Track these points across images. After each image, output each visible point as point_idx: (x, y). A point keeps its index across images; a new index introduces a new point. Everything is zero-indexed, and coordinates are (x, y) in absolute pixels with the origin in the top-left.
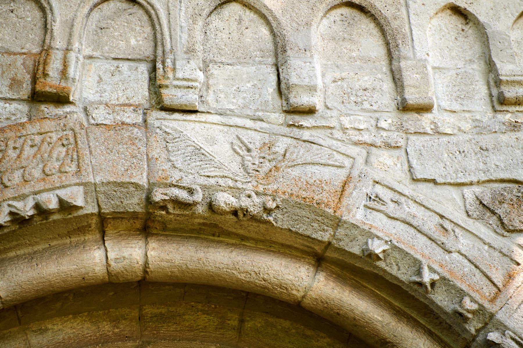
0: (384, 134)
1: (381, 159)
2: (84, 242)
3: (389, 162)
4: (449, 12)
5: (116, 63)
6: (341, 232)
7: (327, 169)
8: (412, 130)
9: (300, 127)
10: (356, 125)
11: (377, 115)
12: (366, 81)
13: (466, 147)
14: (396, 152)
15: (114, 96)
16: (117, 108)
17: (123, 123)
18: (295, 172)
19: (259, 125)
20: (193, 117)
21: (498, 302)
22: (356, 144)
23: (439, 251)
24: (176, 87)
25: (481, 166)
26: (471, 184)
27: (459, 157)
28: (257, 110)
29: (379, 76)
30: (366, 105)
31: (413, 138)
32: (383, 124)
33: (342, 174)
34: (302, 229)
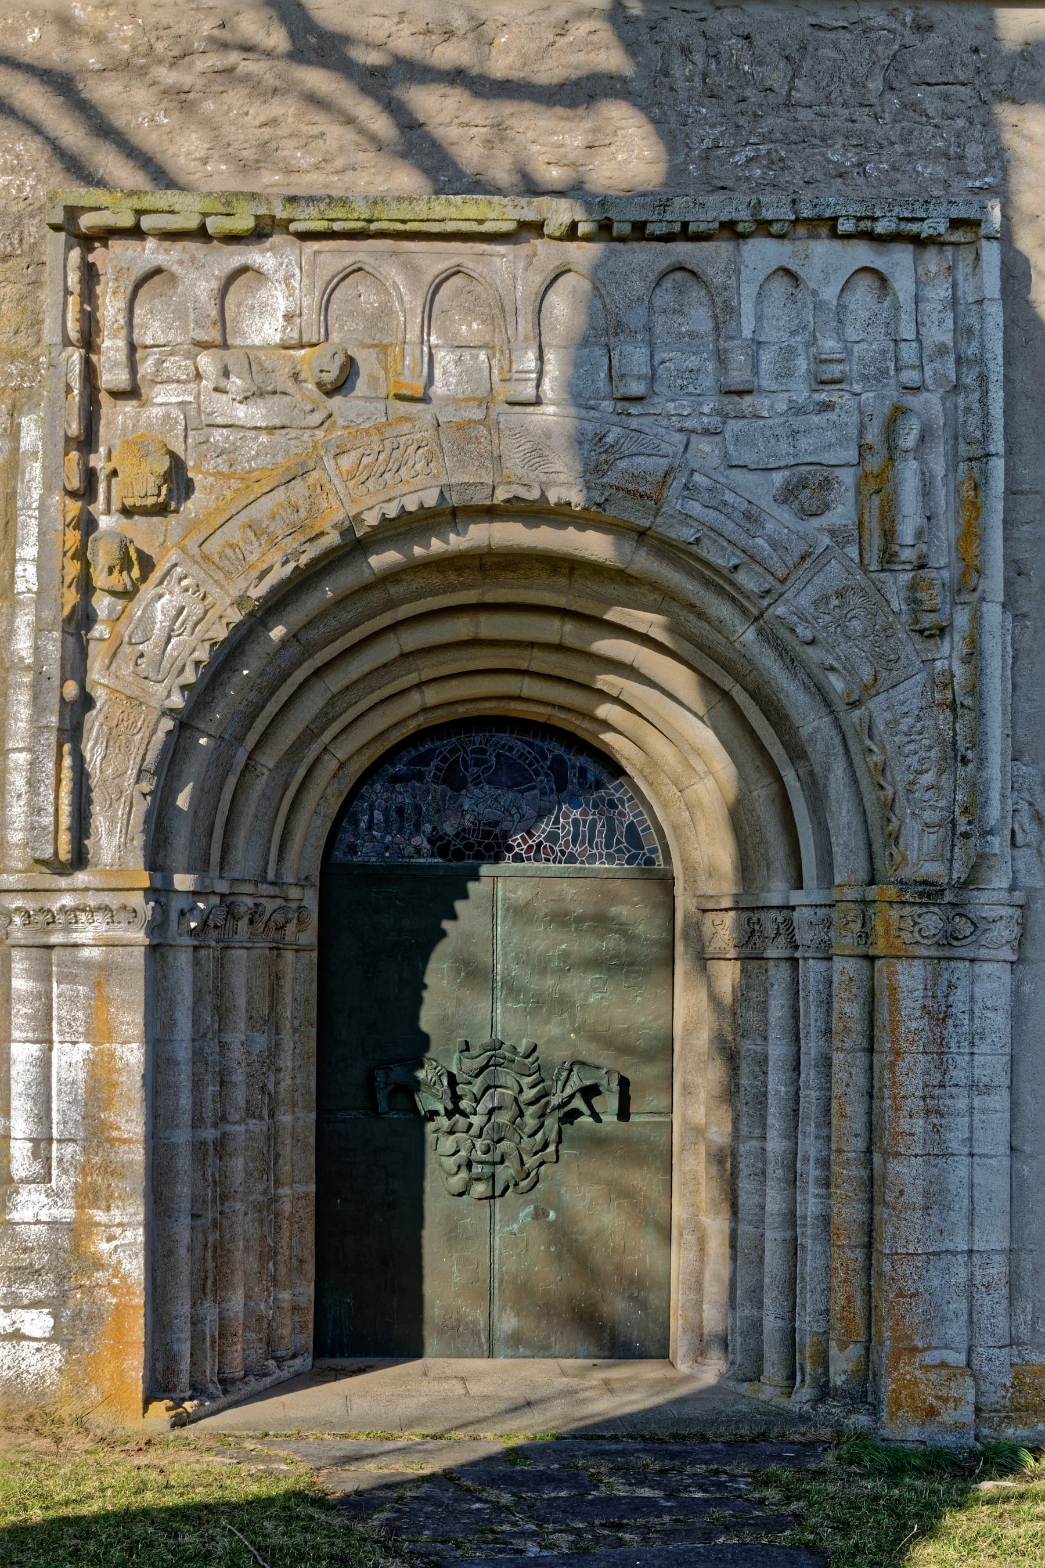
0: (705, 420)
1: (700, 447)
2: (439, 524)
3: (707, 448)
4: (781, 273)
5: (458, 352)
6: (659, 520)
7: (651, 460)
8: (733, 414)
9: (629, 414)
10: (680, 411)
11: (701, 399)
12: (693, 362)
13: (780, 431)
14: (718, 438)
15: (460, 390)
16: (463, 404)
17: (470, 421)
18: (622, 464)
19: (593, 413)
20: (531, 409)
21: (788, 584)
22: (681, 430)
23: (744, 535)
24: (517, 380)
25: (791, 450)
26: (779, 468)
27: (773, 441)
28: (590, 398)
29: (705, 355)
30: (691, 389)
31: (732, 422)
32: (706, 409)
33: (664, 463)
34: (625, 516)
